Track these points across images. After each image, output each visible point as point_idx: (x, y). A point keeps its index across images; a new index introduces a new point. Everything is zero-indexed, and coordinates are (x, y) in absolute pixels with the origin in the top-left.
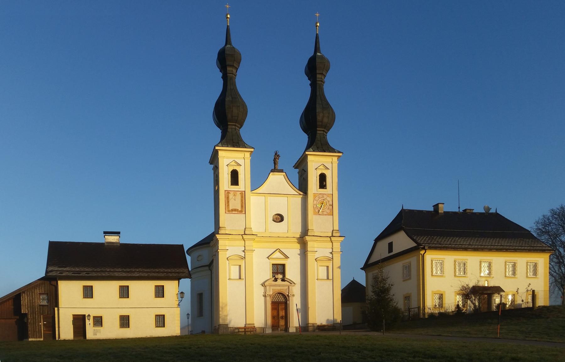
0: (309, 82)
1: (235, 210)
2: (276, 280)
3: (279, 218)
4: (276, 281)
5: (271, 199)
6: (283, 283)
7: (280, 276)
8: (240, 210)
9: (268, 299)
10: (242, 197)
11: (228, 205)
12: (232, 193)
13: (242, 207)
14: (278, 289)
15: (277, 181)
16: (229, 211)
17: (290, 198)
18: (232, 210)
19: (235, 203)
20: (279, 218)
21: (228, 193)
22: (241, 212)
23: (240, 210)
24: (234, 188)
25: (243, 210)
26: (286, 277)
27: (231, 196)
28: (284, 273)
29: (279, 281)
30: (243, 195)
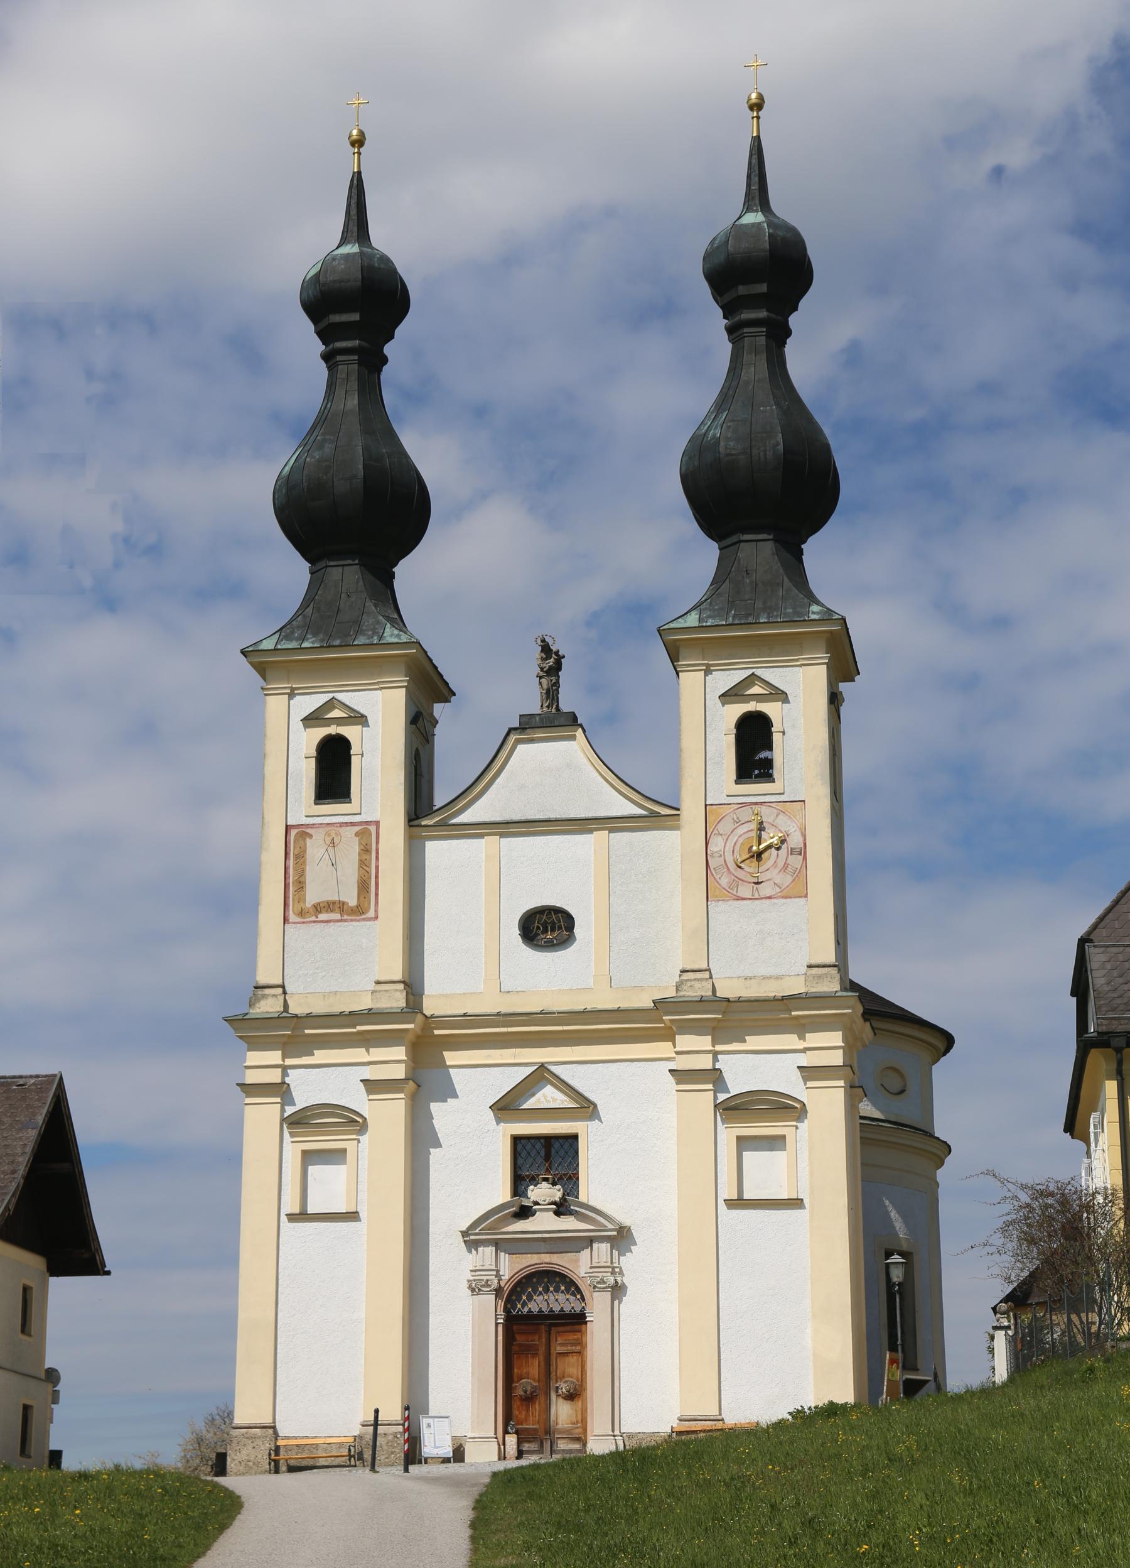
1: (330, 906)
2: (524, 1212)
3: (546, 927)
6: (568, 1224)
8: (353, 902)
9: (489, 1306)
10: (366, 850)
11: (301, 885)
13: (363, 887)
16: (301, 913)
18: (318, 908)
20: (546, 927)
21: (296, 836)
22: (359, 911)
23: (353, 902)
24: (333, 810)
26: (582, 1197)
27: (315, 848)
28: (569, 1179)
30: (368, 834)
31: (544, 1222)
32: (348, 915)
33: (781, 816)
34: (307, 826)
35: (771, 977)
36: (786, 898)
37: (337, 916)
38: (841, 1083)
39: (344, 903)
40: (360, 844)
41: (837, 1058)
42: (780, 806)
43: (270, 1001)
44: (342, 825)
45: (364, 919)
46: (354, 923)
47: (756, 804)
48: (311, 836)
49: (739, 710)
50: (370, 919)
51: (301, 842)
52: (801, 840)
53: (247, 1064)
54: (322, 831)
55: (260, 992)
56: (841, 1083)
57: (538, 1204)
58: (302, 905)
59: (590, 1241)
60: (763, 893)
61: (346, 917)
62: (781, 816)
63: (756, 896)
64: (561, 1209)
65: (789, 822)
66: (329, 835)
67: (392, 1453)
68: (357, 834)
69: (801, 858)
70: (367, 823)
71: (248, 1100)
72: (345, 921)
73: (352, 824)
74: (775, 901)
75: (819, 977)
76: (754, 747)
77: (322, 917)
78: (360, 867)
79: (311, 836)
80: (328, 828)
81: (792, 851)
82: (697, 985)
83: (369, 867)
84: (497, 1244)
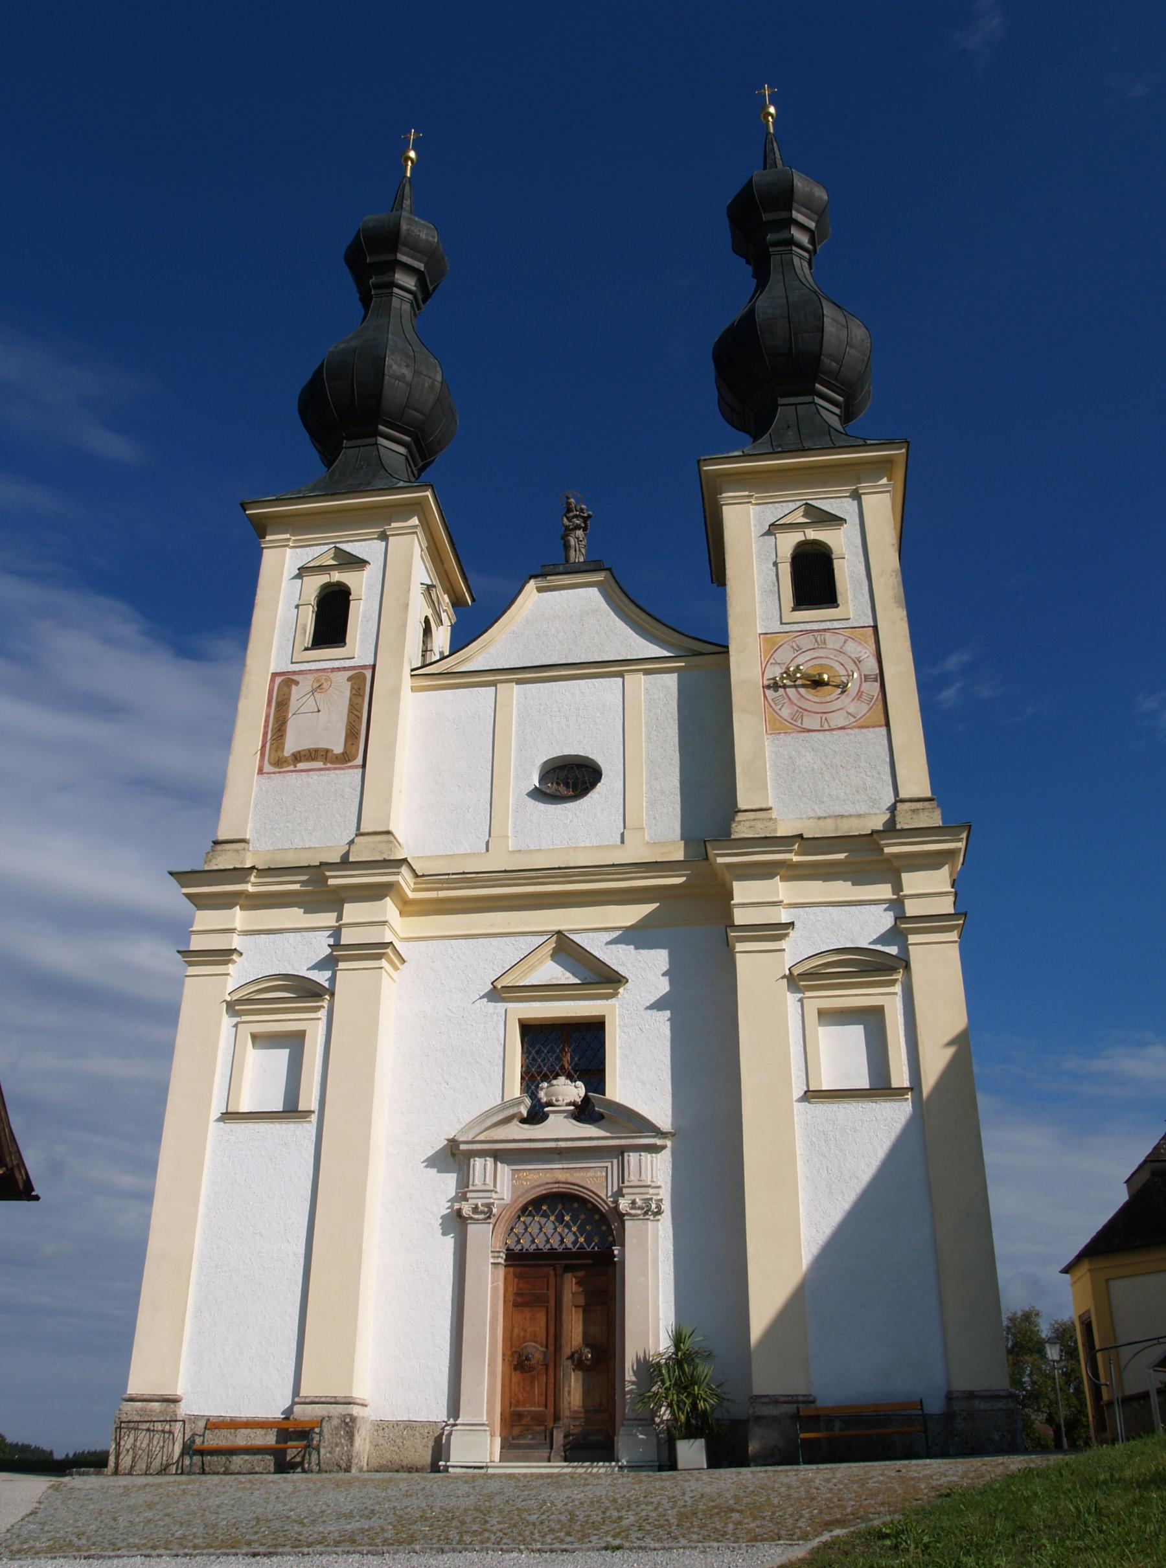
0: (749, 269)
1: (312, 755)
3: (571, 778)
4: (544, 1117)
5: (515, 693)
7: (570, 1091)
8: (338, 749)
12: (306, 684)
13: (352, 734)
14: (556, 1175)
15: (560, 615)
17: (638, 682)
18: (297, 757)
19: (318, 722)
20: (571, 778)
22: (344, 759)
23: (338, 749)
25: (355, 747)
28: (592, 1072)
29: (560, 1128)
30: (362, 684)
31: (560, 1128)
32: (331, 763)
33: (850, 643)
34: (294, 673)
35: (851, 816)
36: (862, 727)
37: (320, 765)
38: (954, 936)
39: (327, 751)
40: (352, 688)
41: (946, 906)
42: (848, 633)
43: (230, 855)
44: (333, 670)
45: (350, 767)
46: (338, 772)
47: (818, 631)
48: (297, 683)
49: (788, 542)
50: (356, 767)
51: (285, 689)
52: (876, 666)
53: (194, 929)
54: (310, 678)
55: (219, 847)
56: (954, 936)
57: (552, 1105)
58: (279, 753)
59: (621, 1151)
60: (833, 724)
61: (329, 765)
62: (850, 643)
63: (826, 727)
64: (584, 1112)
65: (859, 649)
66: (318, 681)
67: (337, 1445)
68: (349, 679)
69: (878, 685)
70: (364, 667)
71: (192, 970)
72: (328, 769)
73: (345, 669)
74: (849, 731)
75: (913, 811)
76: (813, 578)
77: (301, 766)
78: (350, 712)
79: (297, 683)
80: (316, 675)
81: (867, 678)
82: (759, 825)
83: (361, 712)
84: (498, 1156)
